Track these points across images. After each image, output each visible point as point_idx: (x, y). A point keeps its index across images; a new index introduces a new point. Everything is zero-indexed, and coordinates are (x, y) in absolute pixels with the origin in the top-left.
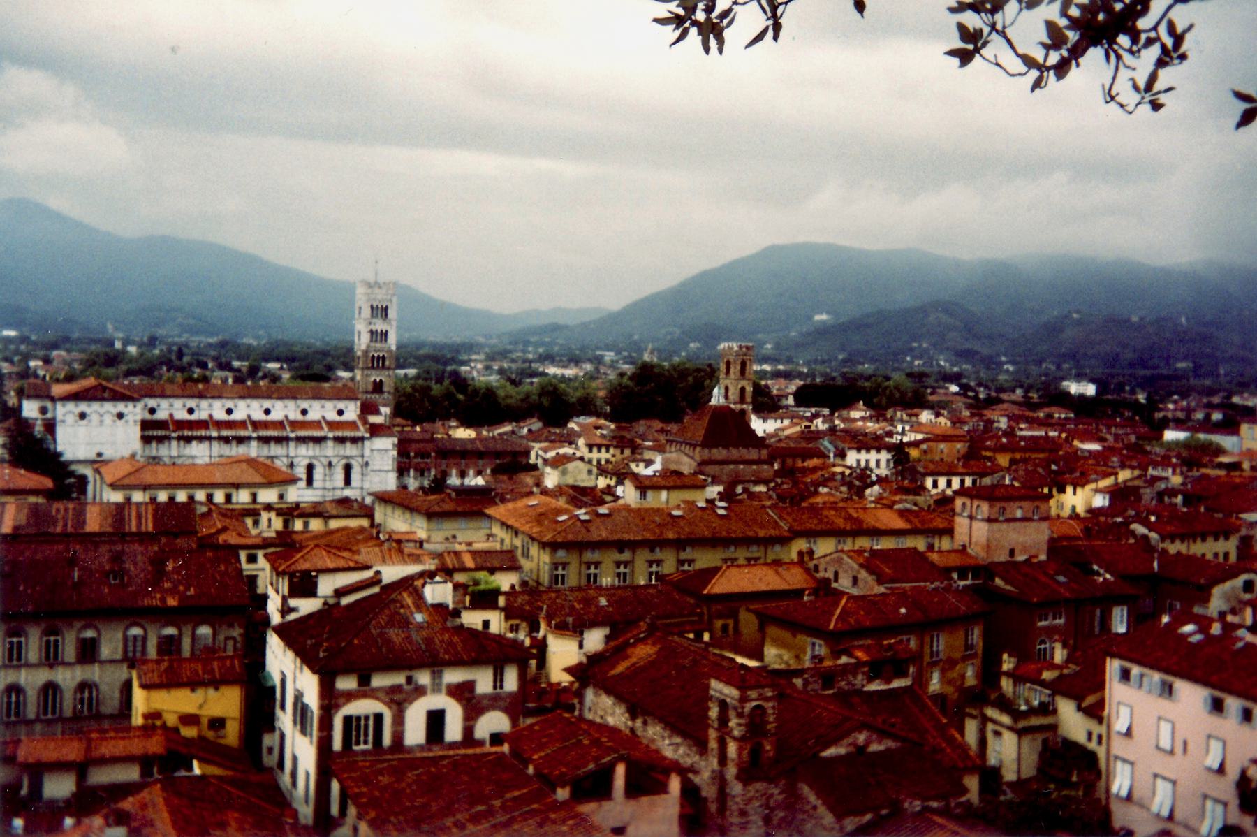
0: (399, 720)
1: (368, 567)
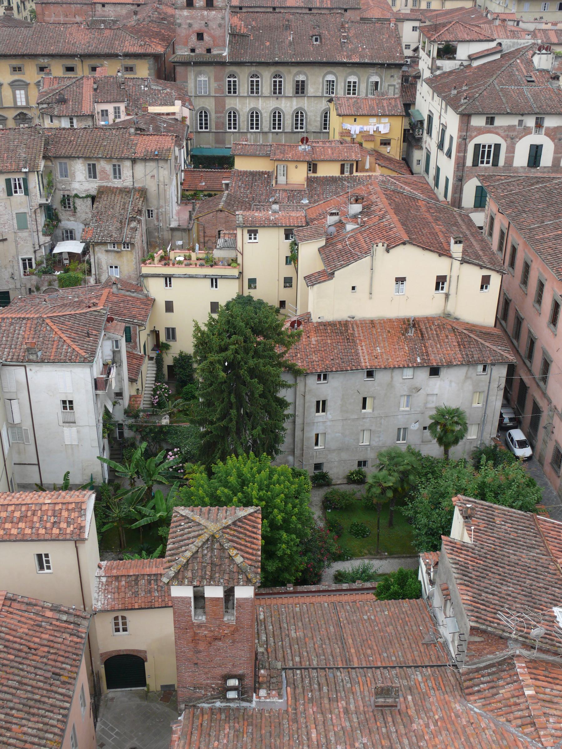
0: (511, 150)
1: (493, 40)
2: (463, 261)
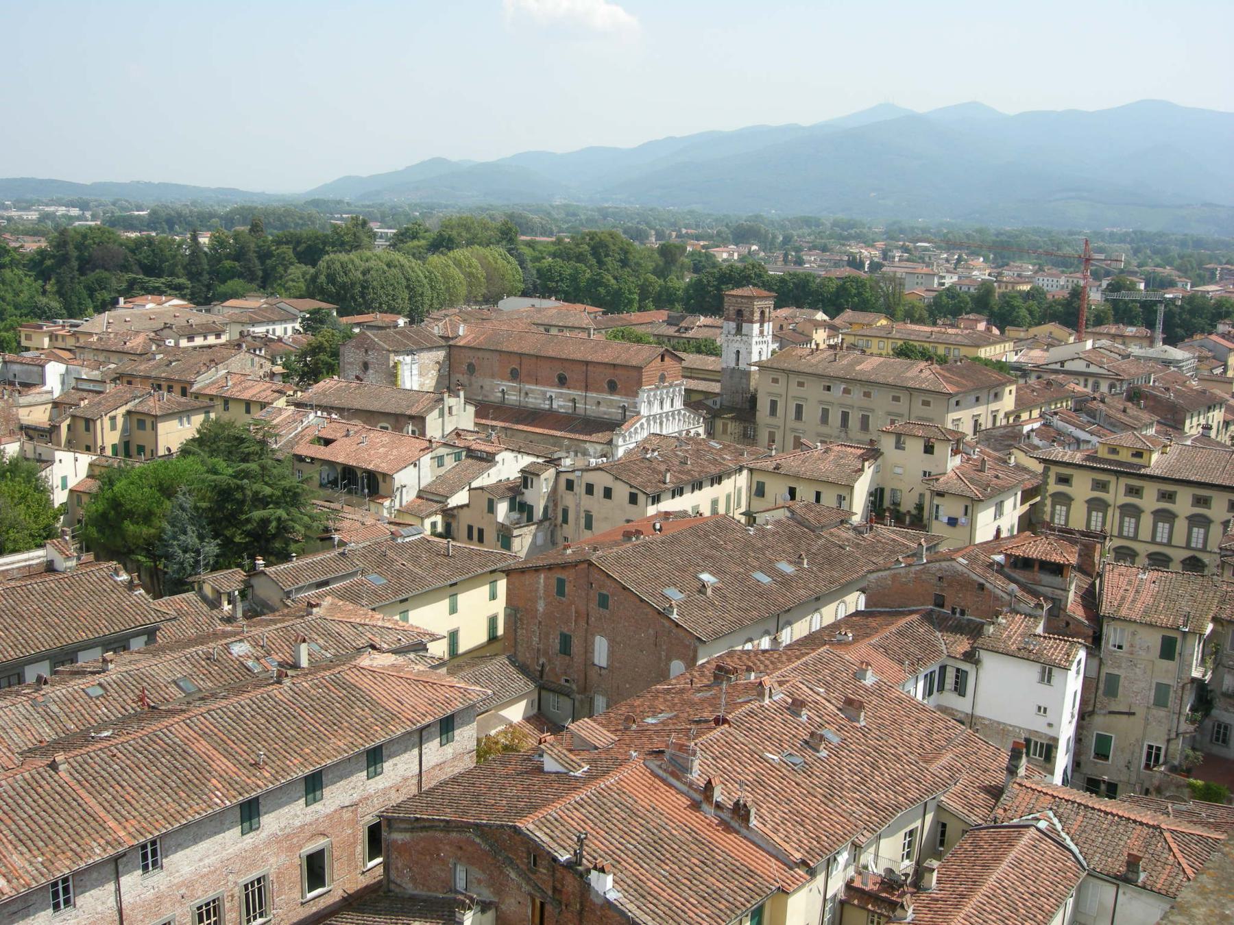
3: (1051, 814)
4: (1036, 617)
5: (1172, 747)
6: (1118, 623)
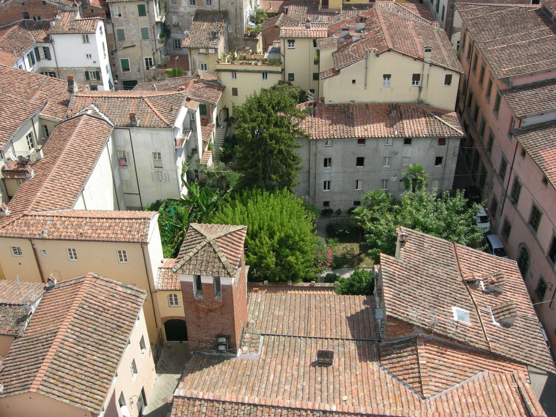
2: (431, 65)
3: (93, 106)
4: (75, 11)
5: (156, 56)
6: (116, 4)
